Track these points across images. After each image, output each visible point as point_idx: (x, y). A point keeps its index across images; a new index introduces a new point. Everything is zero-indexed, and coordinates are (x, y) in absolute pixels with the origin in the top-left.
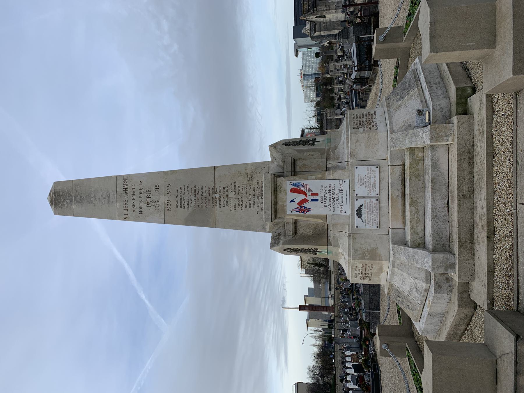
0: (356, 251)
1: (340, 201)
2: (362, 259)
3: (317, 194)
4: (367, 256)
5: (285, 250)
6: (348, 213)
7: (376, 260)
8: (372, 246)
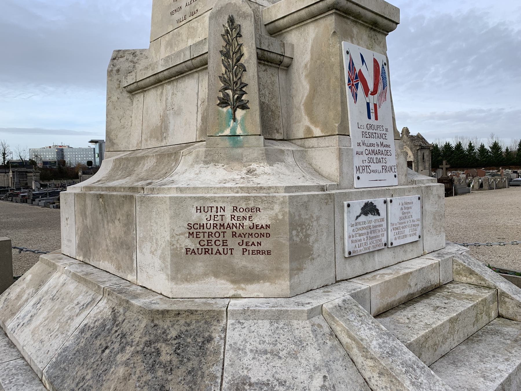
0: (306, 206)
1: (373, 167)
2: (291, 224)
3: (376, 119)
4: (297, 236)
5: (231, 20)
6: (357, 184)
7: (291, 262)
8: (316, 246)
